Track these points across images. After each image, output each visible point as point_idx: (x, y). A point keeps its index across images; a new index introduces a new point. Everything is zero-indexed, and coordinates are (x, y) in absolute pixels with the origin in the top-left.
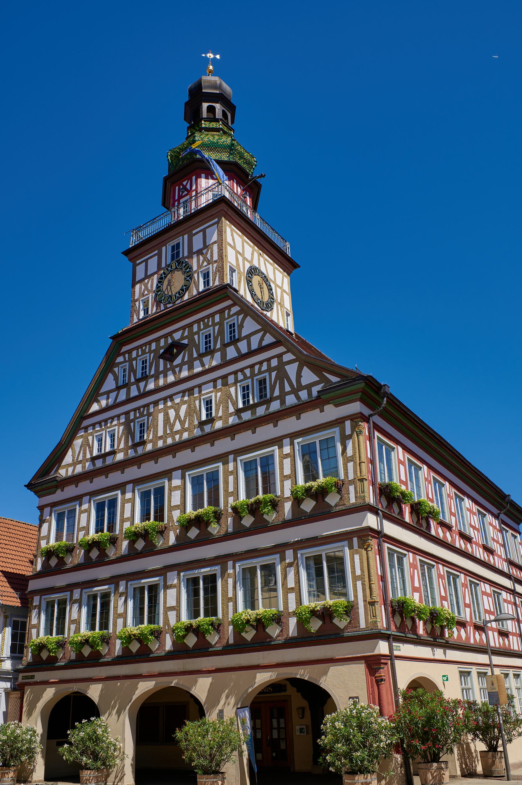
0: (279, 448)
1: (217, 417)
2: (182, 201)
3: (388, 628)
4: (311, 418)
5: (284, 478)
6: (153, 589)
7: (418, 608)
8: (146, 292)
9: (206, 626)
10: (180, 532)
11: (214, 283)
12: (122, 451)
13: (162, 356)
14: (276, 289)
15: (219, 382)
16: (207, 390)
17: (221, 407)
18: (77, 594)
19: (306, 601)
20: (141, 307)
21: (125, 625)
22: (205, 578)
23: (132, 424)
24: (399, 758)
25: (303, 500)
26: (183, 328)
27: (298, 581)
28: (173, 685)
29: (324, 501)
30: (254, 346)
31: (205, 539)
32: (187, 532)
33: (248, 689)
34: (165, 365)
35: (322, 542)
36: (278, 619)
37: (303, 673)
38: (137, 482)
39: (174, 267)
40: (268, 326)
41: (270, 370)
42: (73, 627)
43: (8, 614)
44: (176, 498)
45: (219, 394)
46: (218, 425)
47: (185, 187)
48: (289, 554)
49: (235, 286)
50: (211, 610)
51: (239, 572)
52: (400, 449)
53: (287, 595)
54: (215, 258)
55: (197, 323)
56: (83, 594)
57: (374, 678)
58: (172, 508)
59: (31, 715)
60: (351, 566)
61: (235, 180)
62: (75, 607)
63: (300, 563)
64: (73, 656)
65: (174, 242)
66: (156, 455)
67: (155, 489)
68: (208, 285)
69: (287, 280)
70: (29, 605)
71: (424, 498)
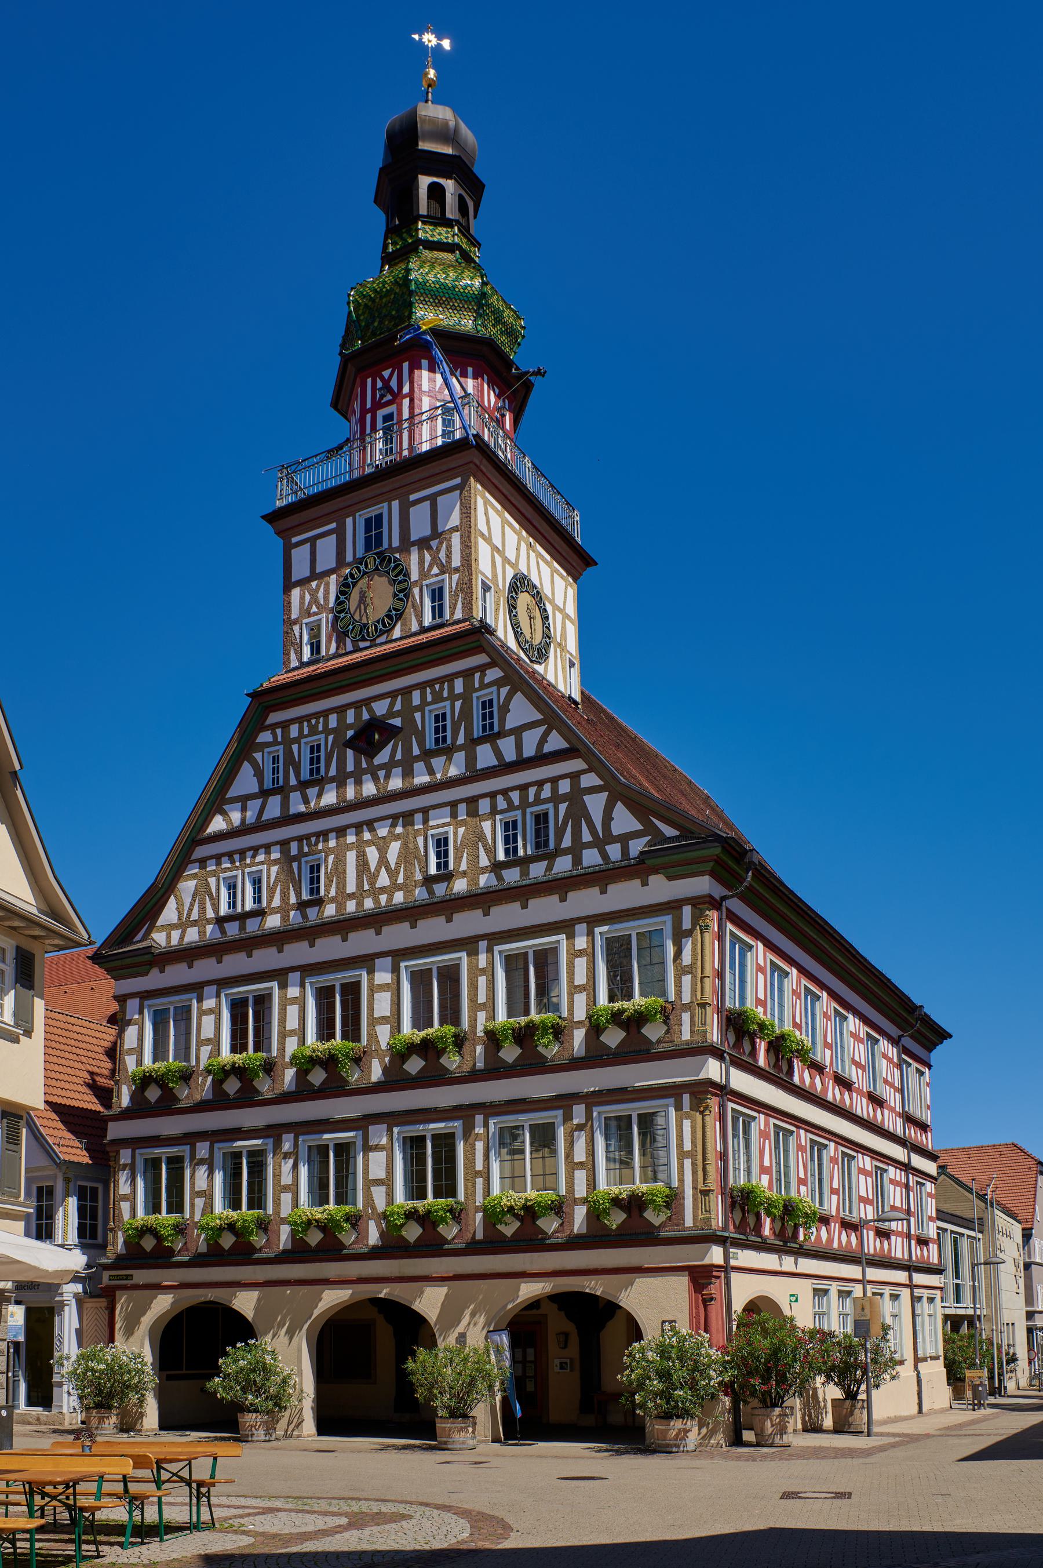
1: (458, 872)
2: (381, 413)
3: (725, 1228)
4: (626, 894)
5: (574, 989)
6: (344, 1151)
7: (769, 1199)
8: (314, 609)
9: (441, 1213)
10: (390, 1061)
11: (452, 614)
12: (277, 912)
13: (350, 744)
14: (554, 615)
15: (462, 808)
16: (439, 820)
17: (465, 855)
18: (202, 1150)
19: (602, 1185)
20: (306, 638)
21: (296, 1204)
22: (435, 1138)
23: (295, 865)
25: (606, 1028)
26: (393, 695)
27: (591, 1153)
28: (382, 1296)
29: (639, 1032)
31: (436, 1076)
32: (403, 1063)
33: (506, 1305)
34: (357, 763)
35: (633, 1096)
36: (558, 1208)
37: (594, 1286)
38: (308, 970)
39: (371, 567)
40: (538, 693)
42: (199, 1203)
43: (70, 1175)
44: (383, 1005)
45: (461, 830)
46: (460, 886)
48: (579, 1112)
50: (446, 1187)
51: (494, 1133)
52: (760, 946)
56: (216, 1150)
58: (374, 1022)
59: (132, 1334)
62: (202, 1172)
63: (596, 1125)
64: (203, 1248)
65: (372, 512)
66: (343, 926)
67: (342, 985)
68: (441, 615)
69: (572, 593)
70: (111, 1163)
71: (788, 1028)
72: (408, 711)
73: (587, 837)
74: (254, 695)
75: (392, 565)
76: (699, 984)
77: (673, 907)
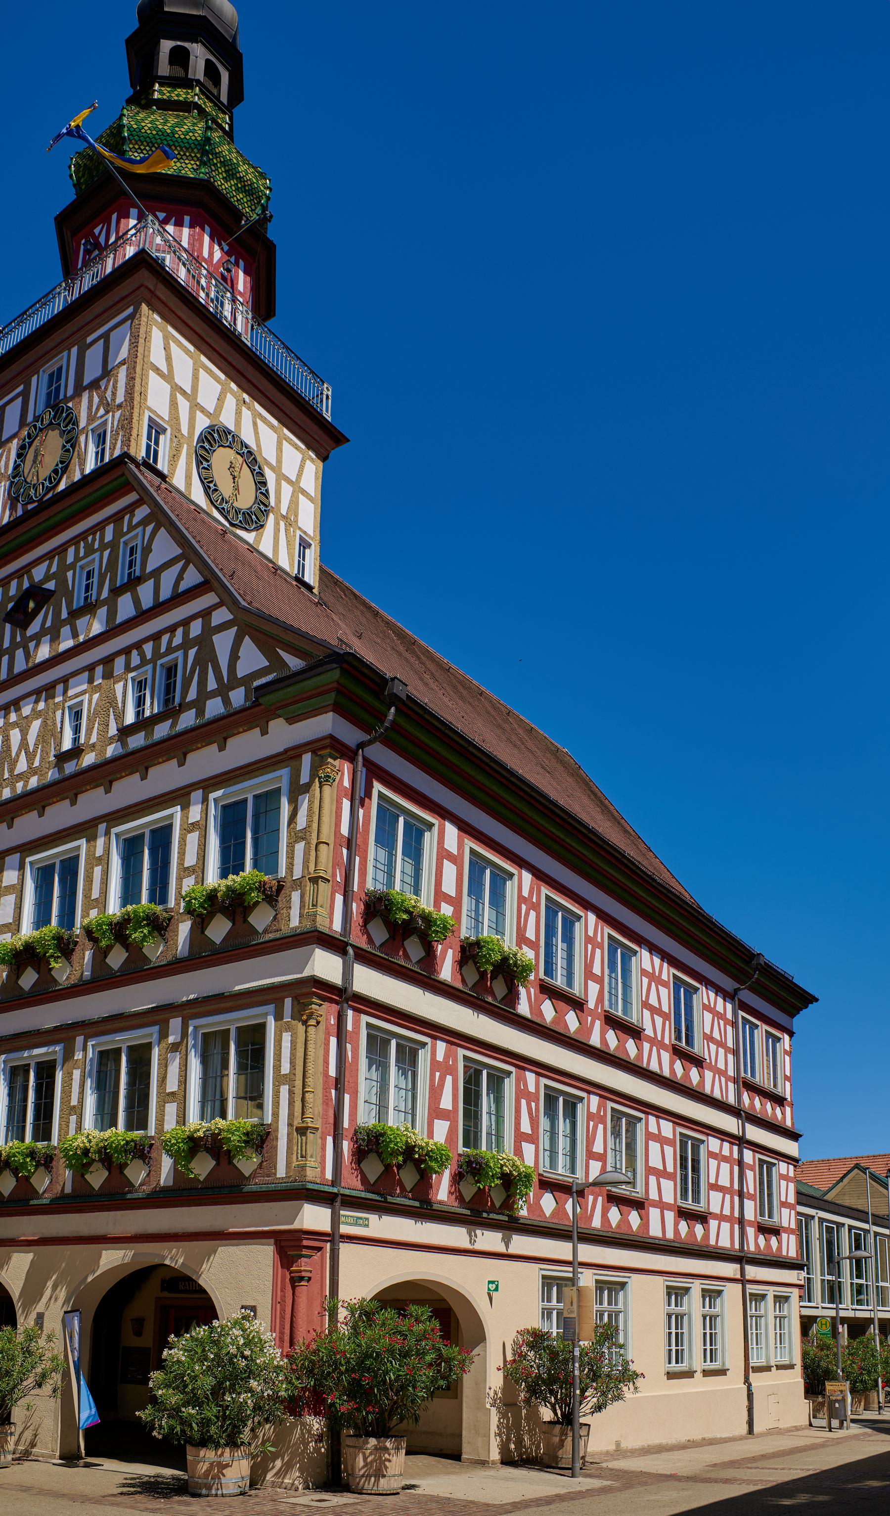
0: (182, 810)
5: (185, 871)
24: (316, 1424)
29: (245, 920)
30: (165, 593)
39: (46, 422)
41: (186, 645)
49: (162, 465)
51: (91, 1060)
53: (164, 1106)
55: (74, 544)
57: (287, 1273)
60: (275, 1054)
61: (207, 228)
63: (191, 1042)
73: (212, 685)
75: (64, 415)
76: (313, 853)
77: (289, 757)
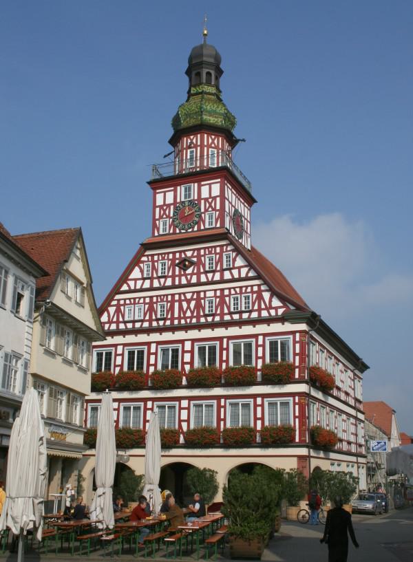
8: (165, 216)
11: (216, 225)
13: (177, 265)
26: (194, 250)
30: (243, 275)
34: (180, 272)
47: (192, 142)
54: (218, 207)
58: (183, 363)
72: (199, 256)
74: (142, 245)
